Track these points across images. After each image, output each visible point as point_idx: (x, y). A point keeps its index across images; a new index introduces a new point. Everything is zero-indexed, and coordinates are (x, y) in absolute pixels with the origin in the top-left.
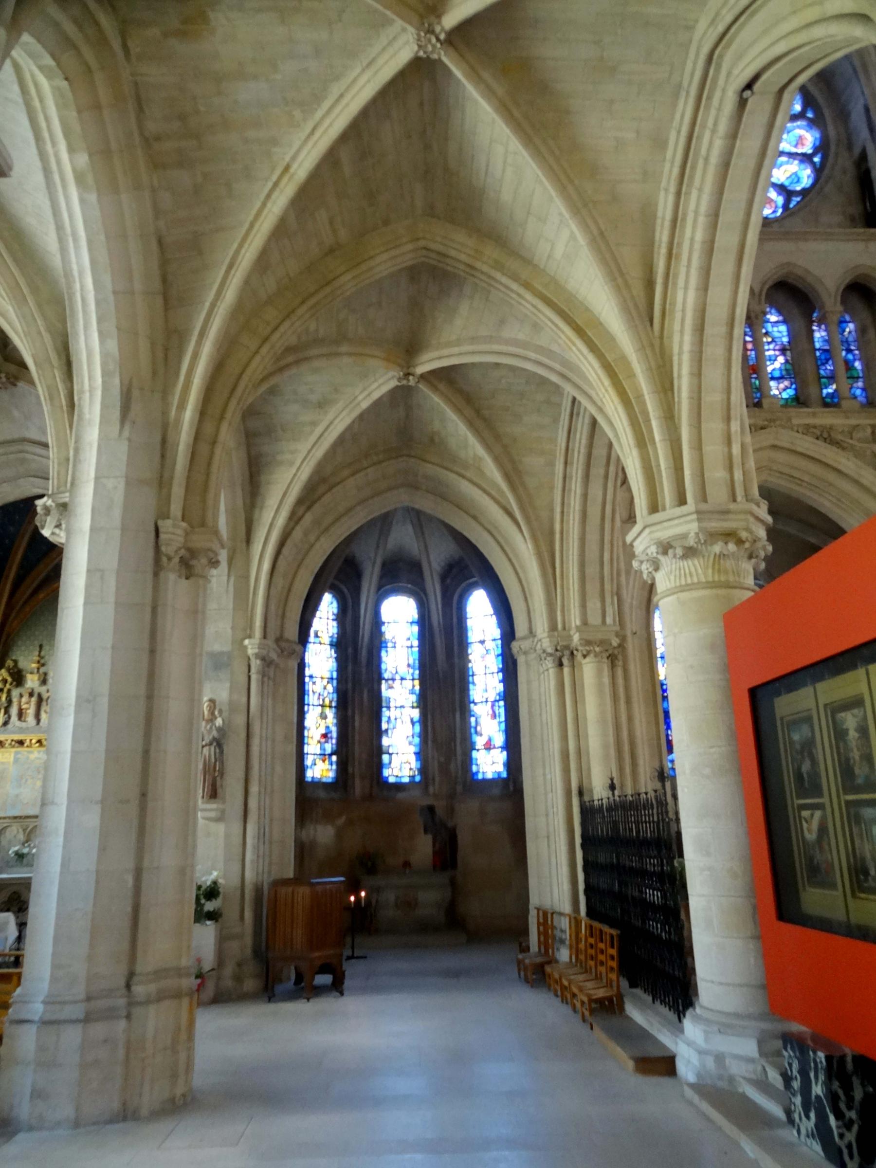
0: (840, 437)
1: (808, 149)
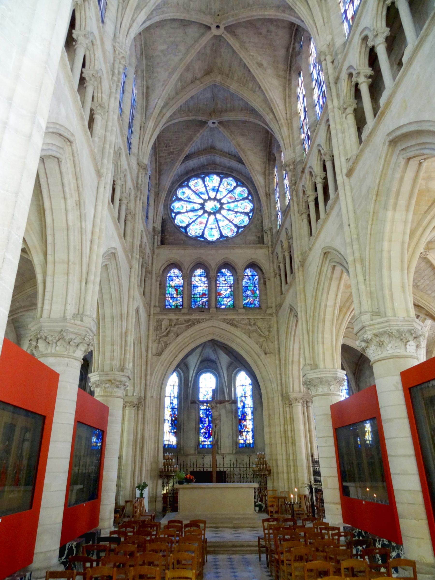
0: (236, 323)
1: (247, 210)
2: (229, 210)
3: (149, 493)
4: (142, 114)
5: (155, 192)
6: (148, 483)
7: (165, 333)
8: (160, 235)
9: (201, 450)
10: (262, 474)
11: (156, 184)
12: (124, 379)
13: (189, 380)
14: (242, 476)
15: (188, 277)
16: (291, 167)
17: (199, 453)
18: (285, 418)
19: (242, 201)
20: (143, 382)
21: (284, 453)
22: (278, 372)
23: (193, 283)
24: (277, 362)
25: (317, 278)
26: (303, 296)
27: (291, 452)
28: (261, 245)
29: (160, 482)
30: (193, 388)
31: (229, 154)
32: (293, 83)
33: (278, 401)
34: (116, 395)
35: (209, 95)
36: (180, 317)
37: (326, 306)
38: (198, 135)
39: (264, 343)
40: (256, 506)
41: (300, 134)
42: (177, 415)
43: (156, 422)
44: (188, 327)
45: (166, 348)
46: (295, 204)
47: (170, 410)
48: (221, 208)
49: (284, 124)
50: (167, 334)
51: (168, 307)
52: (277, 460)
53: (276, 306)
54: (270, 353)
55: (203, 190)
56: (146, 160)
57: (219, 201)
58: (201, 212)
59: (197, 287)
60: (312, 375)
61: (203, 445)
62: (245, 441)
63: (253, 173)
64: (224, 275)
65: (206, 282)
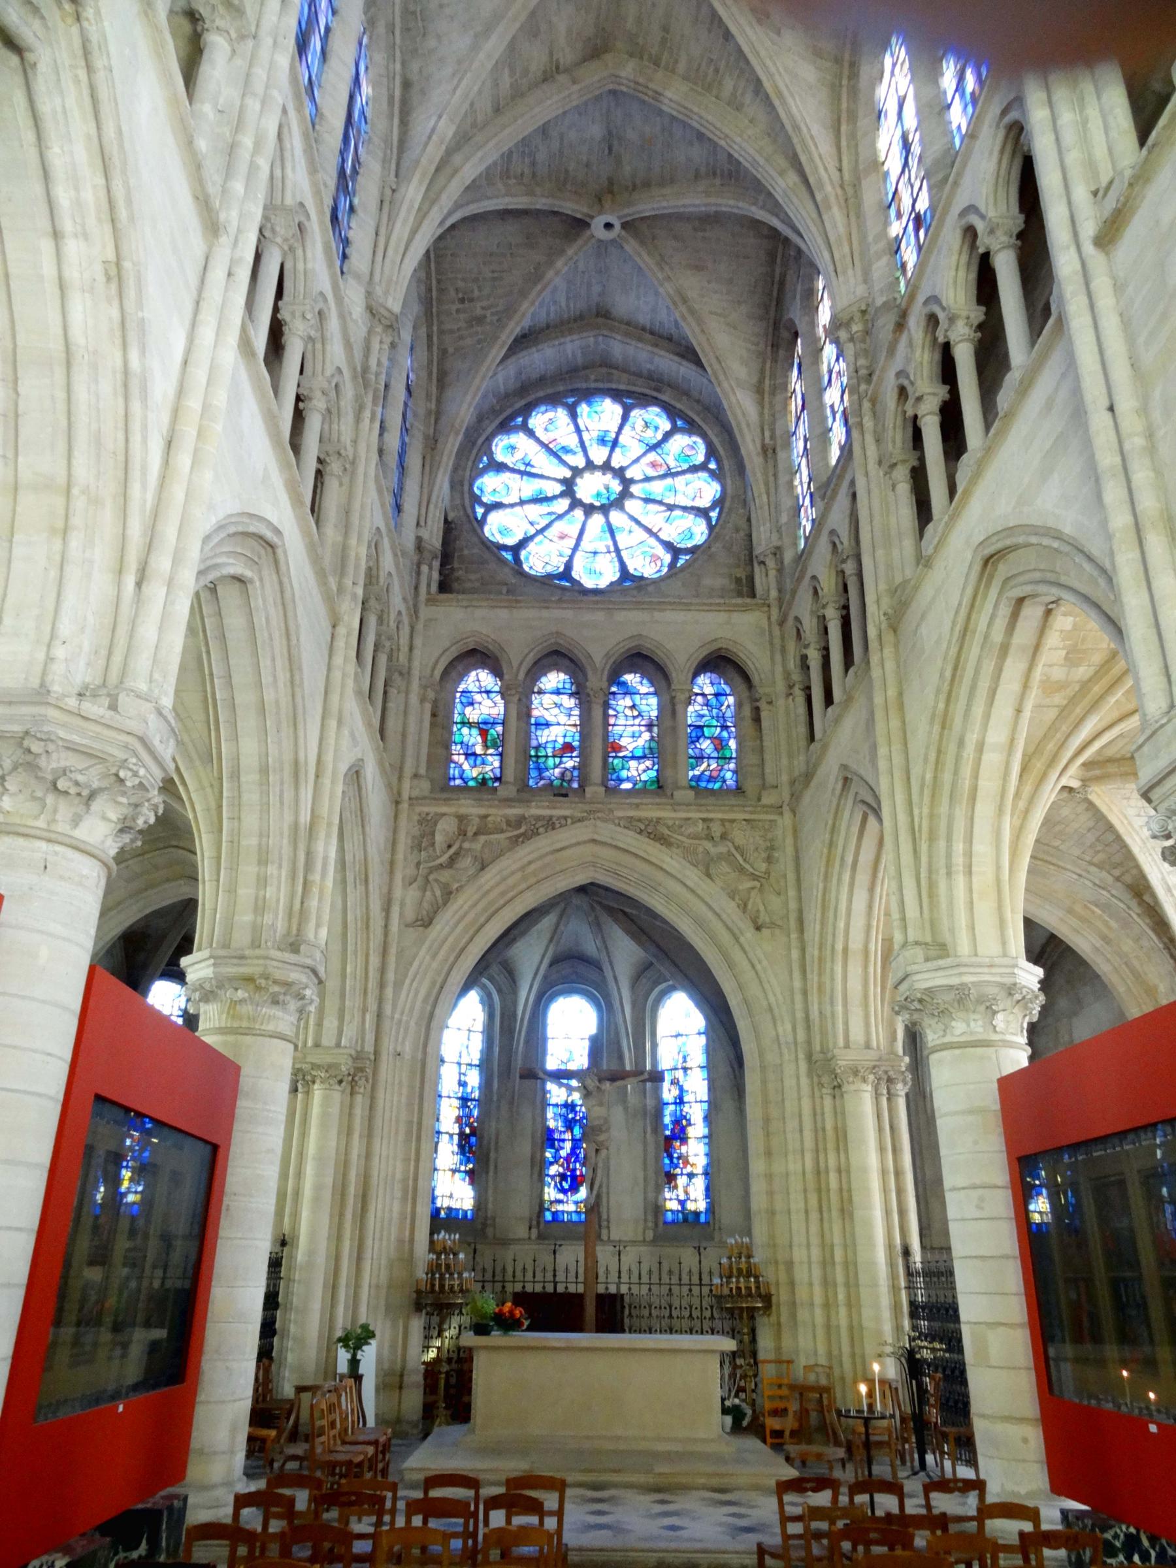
0: (666, 832)
1: (705, 503)
2: (647, 500)
3: (379, 1361)
4: (384, 161)
5: (426, 437)
6: (377, 1326)
7: (444, 859)
8: (436, 564)
9: (550, 1230)
10: (741, 1306)
11: (429, 412)
12: (296, 976)
13: (514, 1015)
14: (675, 1314)
15: (519, 694)
16: (856, 328)
17: (541, 1237)
18: (819, 1131)
19: (689, 476)
20: (372, 1006)
21: (815, 1240)
22: (797, 984)
23: (535, 713)
24: (795, 954)
25: (953, 651)
26: (895, 723)
27: (837, 1240)
28: (748, 600)
29: (417, 1324)
30: (527, 1042)
31: (652, 333)
32: (865, 71)
33: (795, 1078)
34: (271, 1027)
35: (596, 131)
36: (492, 811)
37: (980, 747)
38: (559, 263)
39: (753, 893)
40: (725, 1411)
41: (887, 223)
42: (477, 1120)
43: (409, 1133)
44: (516, 841)
45: (445, 904)
46: (869, 439)
47: (457, 1103)
48: (625, 494)
49: (832, 199)
50: (452, 860)
51: (458, 782)
52: (790, 1264)
53: (792, 783)
54: (773, 925)
55: (572, 441)
56: (396, 297)
57: (619, 473)
58: (564, 504)
59: (547, 725)
60: (927, 978)
61: (555, 1214)
62: (682, 1203)
63: (725, 385)
64: (628, 692)
65: (576, 712)
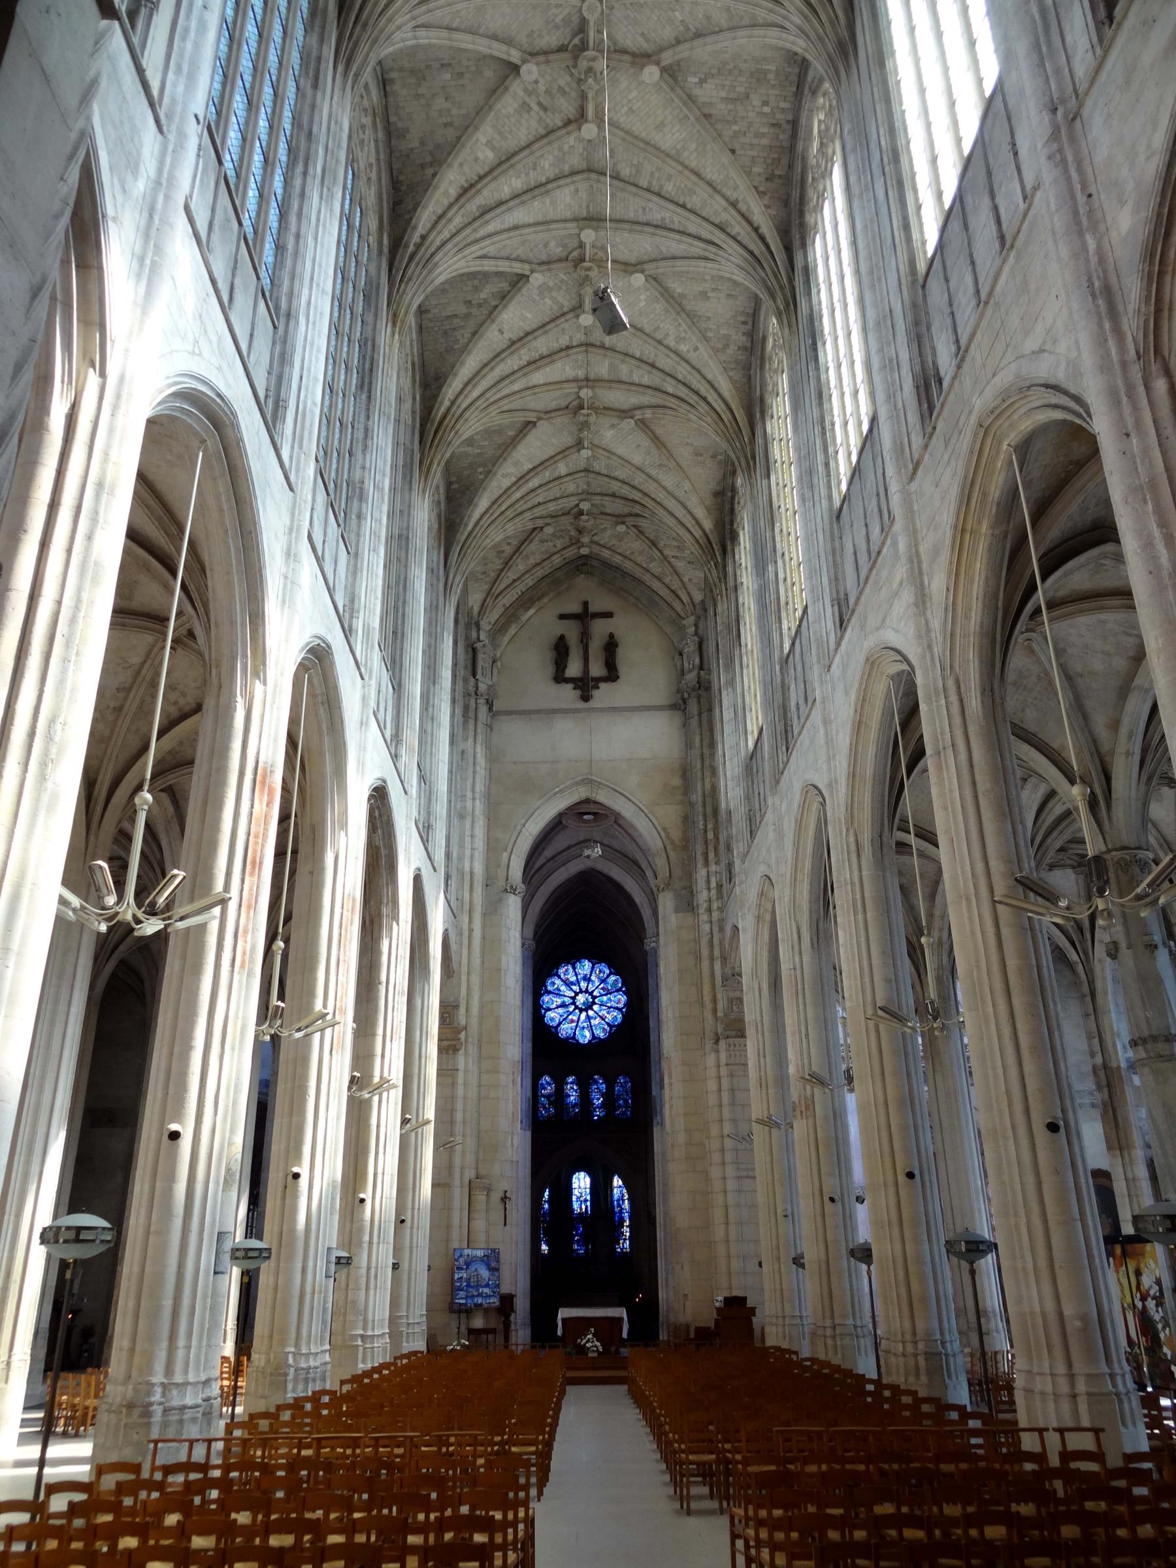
48: (594, 1003)
55: (573, 979)
57: (591, 994)
58: (572, 1008)
64: (596, 1082)
